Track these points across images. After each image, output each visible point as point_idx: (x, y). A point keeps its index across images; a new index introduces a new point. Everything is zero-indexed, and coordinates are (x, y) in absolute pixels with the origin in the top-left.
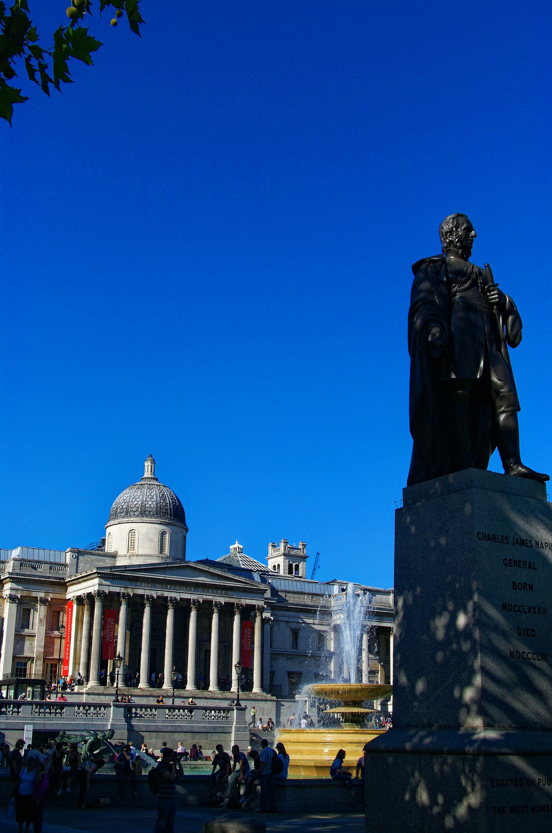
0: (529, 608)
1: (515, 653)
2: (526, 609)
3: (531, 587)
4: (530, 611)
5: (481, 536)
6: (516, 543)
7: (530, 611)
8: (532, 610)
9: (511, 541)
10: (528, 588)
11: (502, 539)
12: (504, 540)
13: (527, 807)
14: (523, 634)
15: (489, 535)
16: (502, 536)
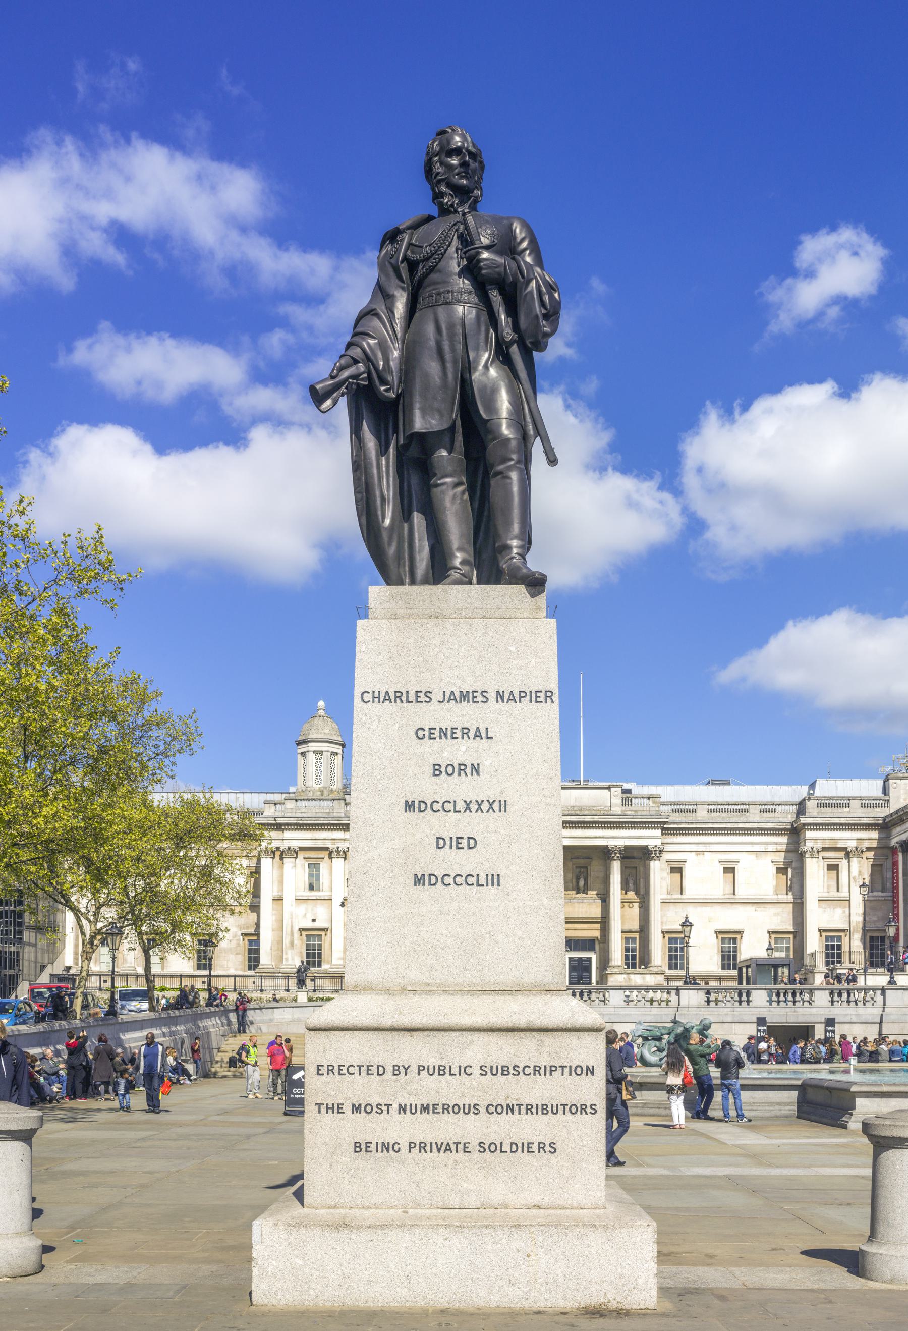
0: (468, 804)
1: (427, 878)
2: (461, 806)
3: (476, 770)
4: (468, 808)
5: (368, 697)
6: (450, 699)
7: (468, 808)
8: (474, 807)
9: (437, 696)
10: (468, 771)
11: (417, 697)
12: (423, 697)
13: (389, 1106)
14: (447, 846)
15: (387, 692)
16: (417, 692)
